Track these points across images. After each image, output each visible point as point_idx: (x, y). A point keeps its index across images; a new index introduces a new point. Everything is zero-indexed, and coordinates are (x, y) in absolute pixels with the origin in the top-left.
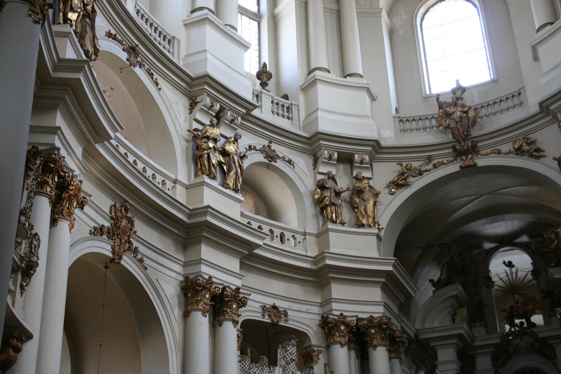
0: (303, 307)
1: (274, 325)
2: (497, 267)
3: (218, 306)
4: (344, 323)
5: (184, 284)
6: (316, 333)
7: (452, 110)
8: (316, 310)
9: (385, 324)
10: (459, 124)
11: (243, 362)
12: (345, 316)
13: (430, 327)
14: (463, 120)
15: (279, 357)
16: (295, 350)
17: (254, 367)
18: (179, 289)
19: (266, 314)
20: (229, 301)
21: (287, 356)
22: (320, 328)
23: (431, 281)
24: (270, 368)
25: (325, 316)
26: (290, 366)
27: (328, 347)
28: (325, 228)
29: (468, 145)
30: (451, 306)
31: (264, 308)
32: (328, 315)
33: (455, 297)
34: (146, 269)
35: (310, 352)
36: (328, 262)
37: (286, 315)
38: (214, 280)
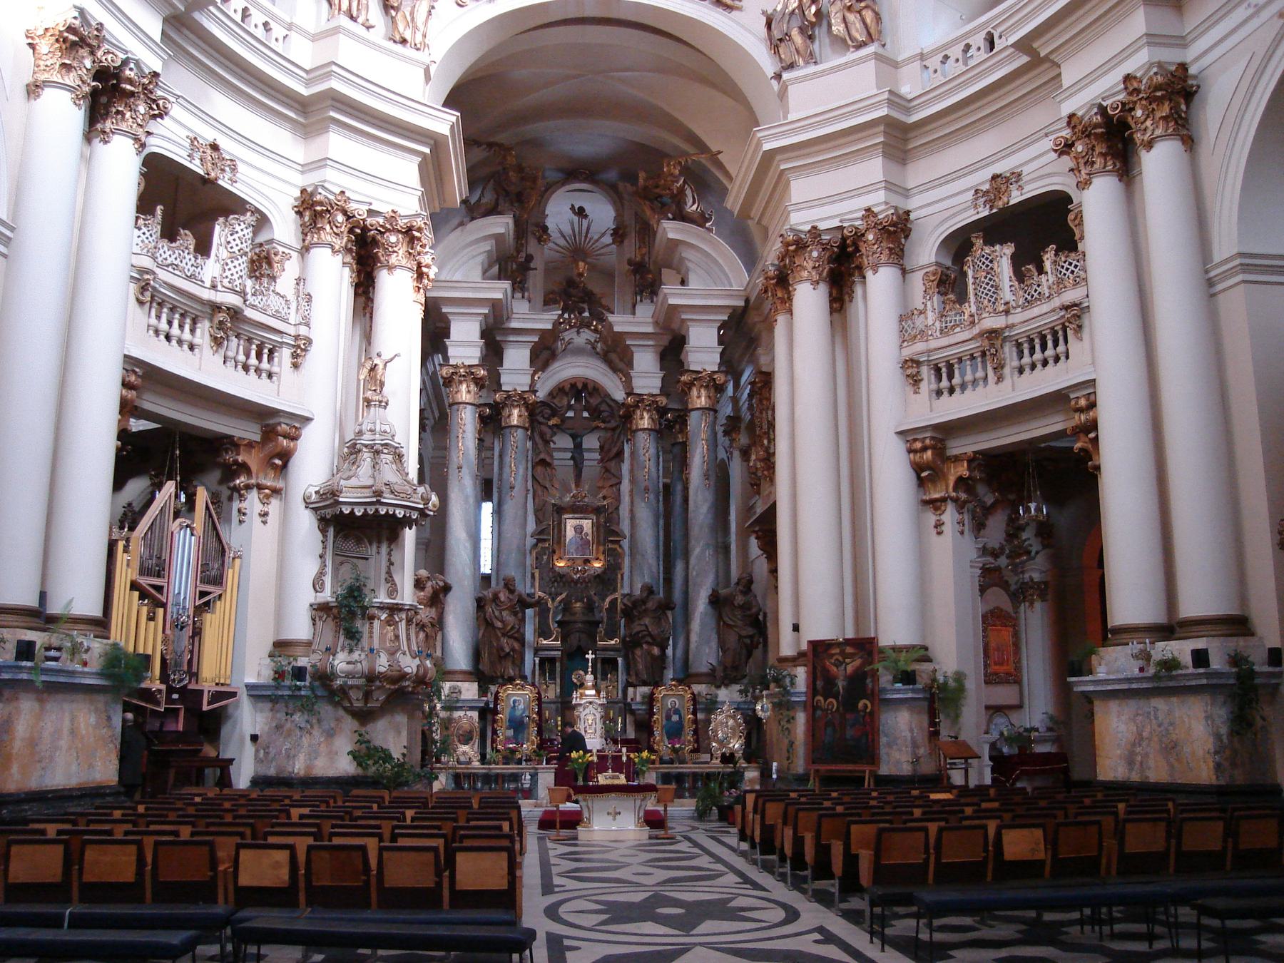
1: (207, 182)
2: (558, 213)
4: (345, 213)
9: (419, 230)
11: (144, 230)
19: (197, 155)
20: (132, 94)
21: (233, 244)
24: (196, 258)
25: (309, 190)
26: (236, 263)
27: (305, 250)
28: (333, 24)
33: (498, 238)
37: (234, 169)
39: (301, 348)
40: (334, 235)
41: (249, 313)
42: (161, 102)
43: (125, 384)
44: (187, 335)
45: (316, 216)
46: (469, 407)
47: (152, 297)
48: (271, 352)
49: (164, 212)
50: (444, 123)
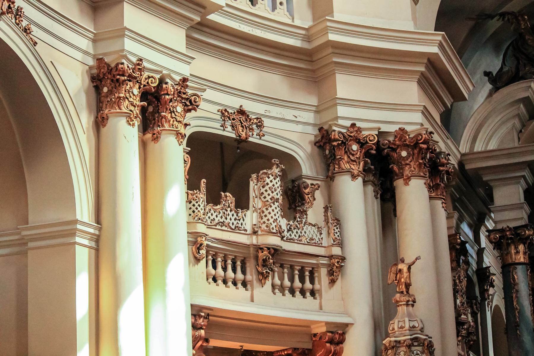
0: (289, 114)
1: (240, 141)
3: (151, 109)
5: (95, 71)
6: (311, 156)
8: (309, 117)
9: (426, 142)
12: (359, 128)
13: (483, 149)
15: (252, 194)
16: (279, 183)
17: (212, 211)
18: (87, 81)
19: (228, 123)
20: (171, 100)
21: (266, 194)
22: (316, 148)
23: (487, 74)
25: (326, 127)
26: (270, 209)
27: (330, 178)
30: (518, 115)
31: (224, 114)
32: (330, 126)
34: (35, 44)
35: (299, 186)
36: (333, 37)
37: (260, 126)
38: (145, 64)
39: (336, 267)
40: (352, 163)
41: (287, 246)
42: (193, 98)
43: (195, 327)
44: (240, 276)
45: (333, 150)
46: (519, 267)
47: (207, 252)
48: (312, 273)
49: (207, 184)
50: (432, 44)
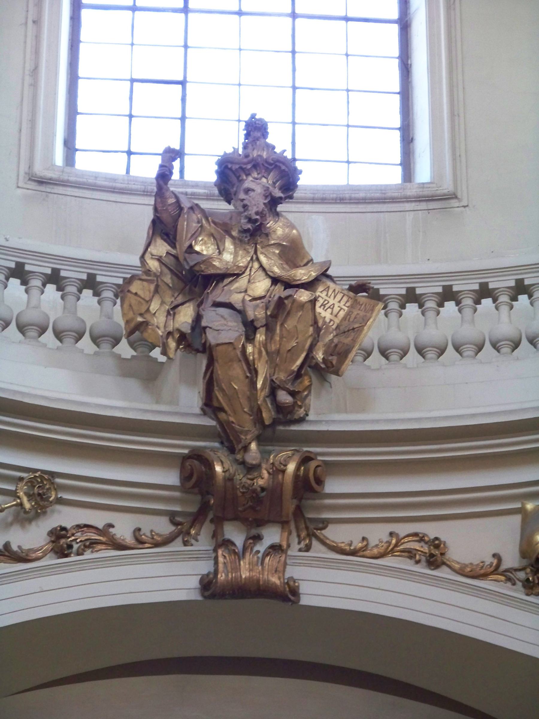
7: (227, 257)
10: (260, 337)
14: (290, 324)
29: (278, 471)
